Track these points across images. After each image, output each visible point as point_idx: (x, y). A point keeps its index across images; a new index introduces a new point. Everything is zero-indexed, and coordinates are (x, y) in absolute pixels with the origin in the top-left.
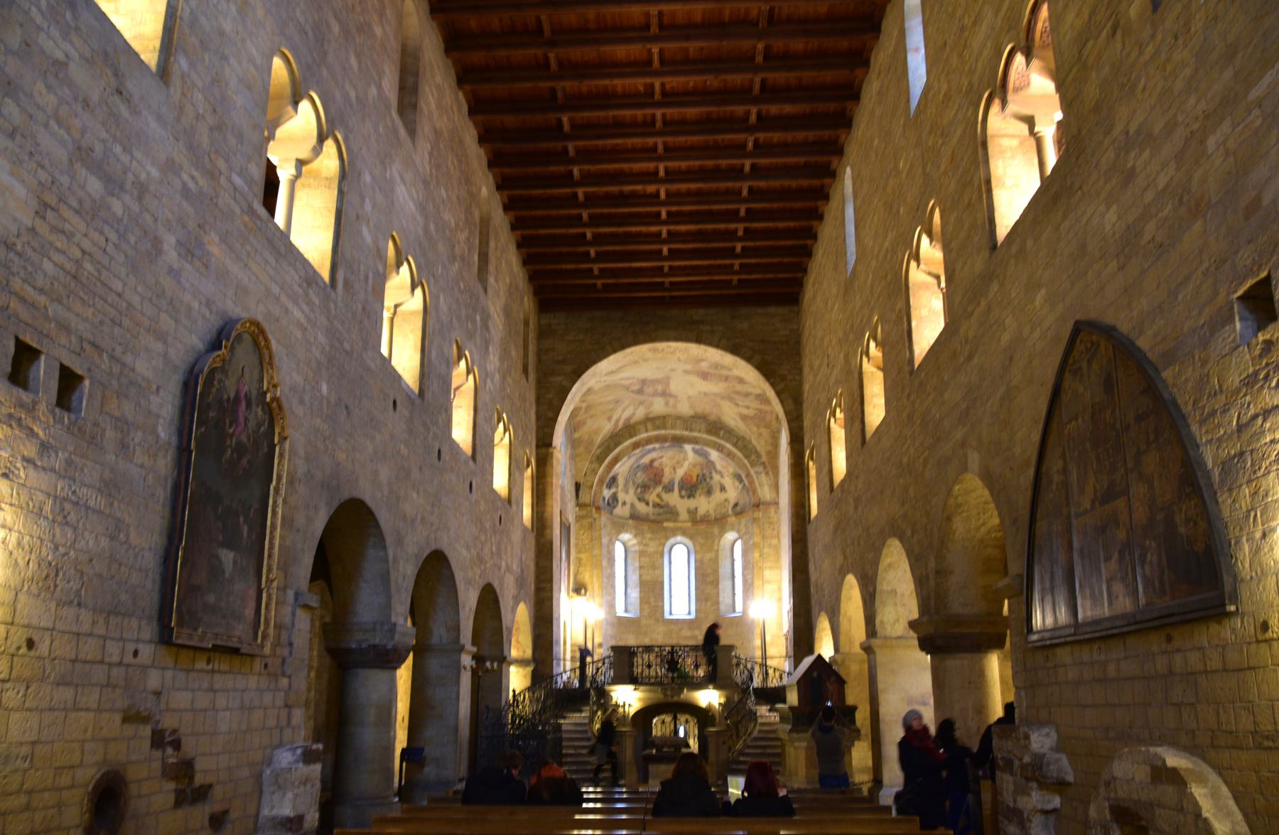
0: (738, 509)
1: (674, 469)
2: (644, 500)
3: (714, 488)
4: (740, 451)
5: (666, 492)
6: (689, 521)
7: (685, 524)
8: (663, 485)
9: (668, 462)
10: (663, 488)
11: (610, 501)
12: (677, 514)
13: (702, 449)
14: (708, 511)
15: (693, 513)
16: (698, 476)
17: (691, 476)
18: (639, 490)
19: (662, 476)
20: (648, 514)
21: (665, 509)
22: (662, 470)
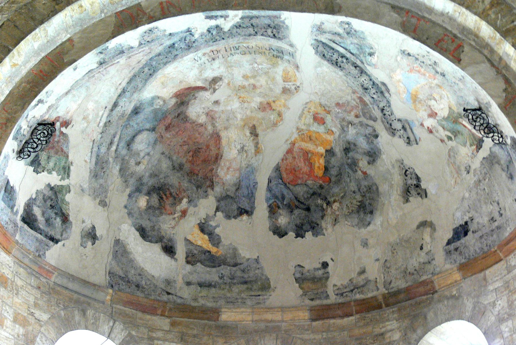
0: (470, 239)
1: (254, 133)
2: (159, 239)
3: (383, 188)
4: (483, 15)
5: (228, 217)
6: (296, 308)
7: (288, 316)
8: (218, 189)
9: (235, 105)
10: (219, 200)
11: (37, 211)
12: (266, 287)
13: (350, 32)
14: (363, 272)
15: (314, 280)
16: (330, 152)
17: (306, 154)
18: (143, 202)
19: (218, 158)
20: (168, 282)
21: (226, 270)
22: (217, 137)
